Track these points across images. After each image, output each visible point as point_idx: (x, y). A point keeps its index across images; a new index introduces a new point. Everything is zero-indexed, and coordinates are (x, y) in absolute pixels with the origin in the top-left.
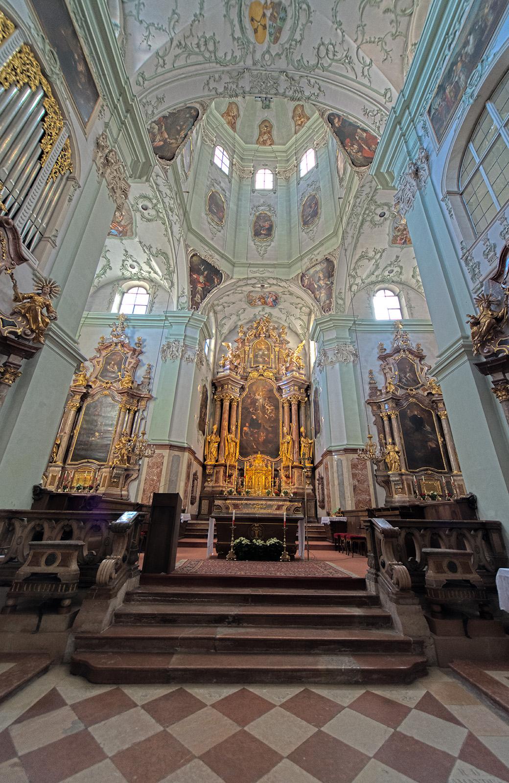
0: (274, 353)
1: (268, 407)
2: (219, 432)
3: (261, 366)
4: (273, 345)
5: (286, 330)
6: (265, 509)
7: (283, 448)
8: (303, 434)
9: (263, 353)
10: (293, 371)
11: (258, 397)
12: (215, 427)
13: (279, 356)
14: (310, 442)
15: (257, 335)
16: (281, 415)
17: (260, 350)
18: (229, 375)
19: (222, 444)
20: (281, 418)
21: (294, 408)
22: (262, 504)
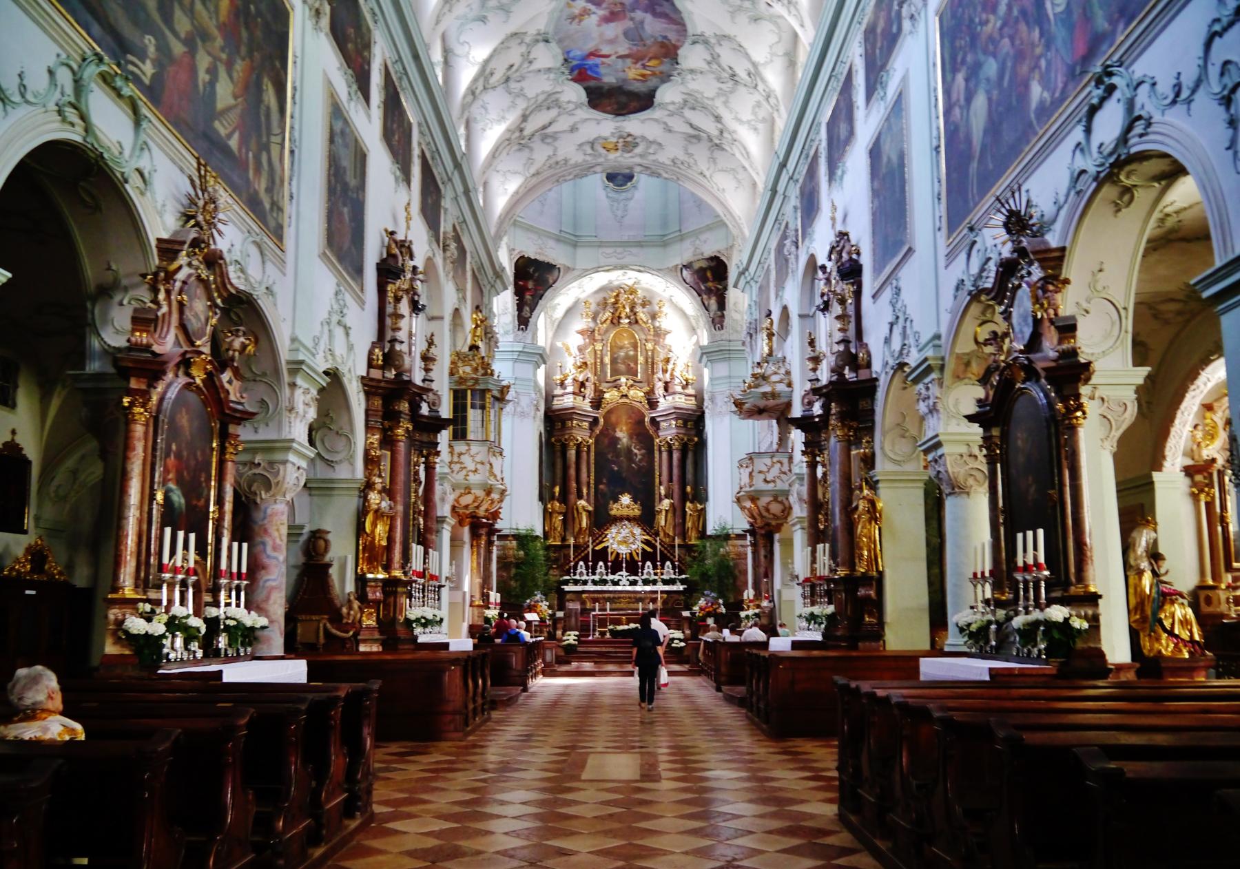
0: (644, 352)
1: (636, 451)
2: (564, 498)
3: (623, 380)
4: (643, 337)
5: (667, 305)
6: (633, 603)
7: (661, 520)
8: (690, 497)
9: (627, 354)
10: (674, 393)
11: (619, 434)
12: (557, 489)
13: (653, 359)
14: (699, 507)
15: (615, 321)
16: (657, 464)
17: (621, 348)
18: (573, 408)
19: (570, 516)
20: (657, 468)
21: (676, 455)
22: (630, 598)
